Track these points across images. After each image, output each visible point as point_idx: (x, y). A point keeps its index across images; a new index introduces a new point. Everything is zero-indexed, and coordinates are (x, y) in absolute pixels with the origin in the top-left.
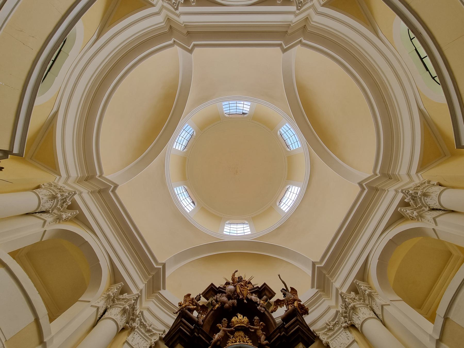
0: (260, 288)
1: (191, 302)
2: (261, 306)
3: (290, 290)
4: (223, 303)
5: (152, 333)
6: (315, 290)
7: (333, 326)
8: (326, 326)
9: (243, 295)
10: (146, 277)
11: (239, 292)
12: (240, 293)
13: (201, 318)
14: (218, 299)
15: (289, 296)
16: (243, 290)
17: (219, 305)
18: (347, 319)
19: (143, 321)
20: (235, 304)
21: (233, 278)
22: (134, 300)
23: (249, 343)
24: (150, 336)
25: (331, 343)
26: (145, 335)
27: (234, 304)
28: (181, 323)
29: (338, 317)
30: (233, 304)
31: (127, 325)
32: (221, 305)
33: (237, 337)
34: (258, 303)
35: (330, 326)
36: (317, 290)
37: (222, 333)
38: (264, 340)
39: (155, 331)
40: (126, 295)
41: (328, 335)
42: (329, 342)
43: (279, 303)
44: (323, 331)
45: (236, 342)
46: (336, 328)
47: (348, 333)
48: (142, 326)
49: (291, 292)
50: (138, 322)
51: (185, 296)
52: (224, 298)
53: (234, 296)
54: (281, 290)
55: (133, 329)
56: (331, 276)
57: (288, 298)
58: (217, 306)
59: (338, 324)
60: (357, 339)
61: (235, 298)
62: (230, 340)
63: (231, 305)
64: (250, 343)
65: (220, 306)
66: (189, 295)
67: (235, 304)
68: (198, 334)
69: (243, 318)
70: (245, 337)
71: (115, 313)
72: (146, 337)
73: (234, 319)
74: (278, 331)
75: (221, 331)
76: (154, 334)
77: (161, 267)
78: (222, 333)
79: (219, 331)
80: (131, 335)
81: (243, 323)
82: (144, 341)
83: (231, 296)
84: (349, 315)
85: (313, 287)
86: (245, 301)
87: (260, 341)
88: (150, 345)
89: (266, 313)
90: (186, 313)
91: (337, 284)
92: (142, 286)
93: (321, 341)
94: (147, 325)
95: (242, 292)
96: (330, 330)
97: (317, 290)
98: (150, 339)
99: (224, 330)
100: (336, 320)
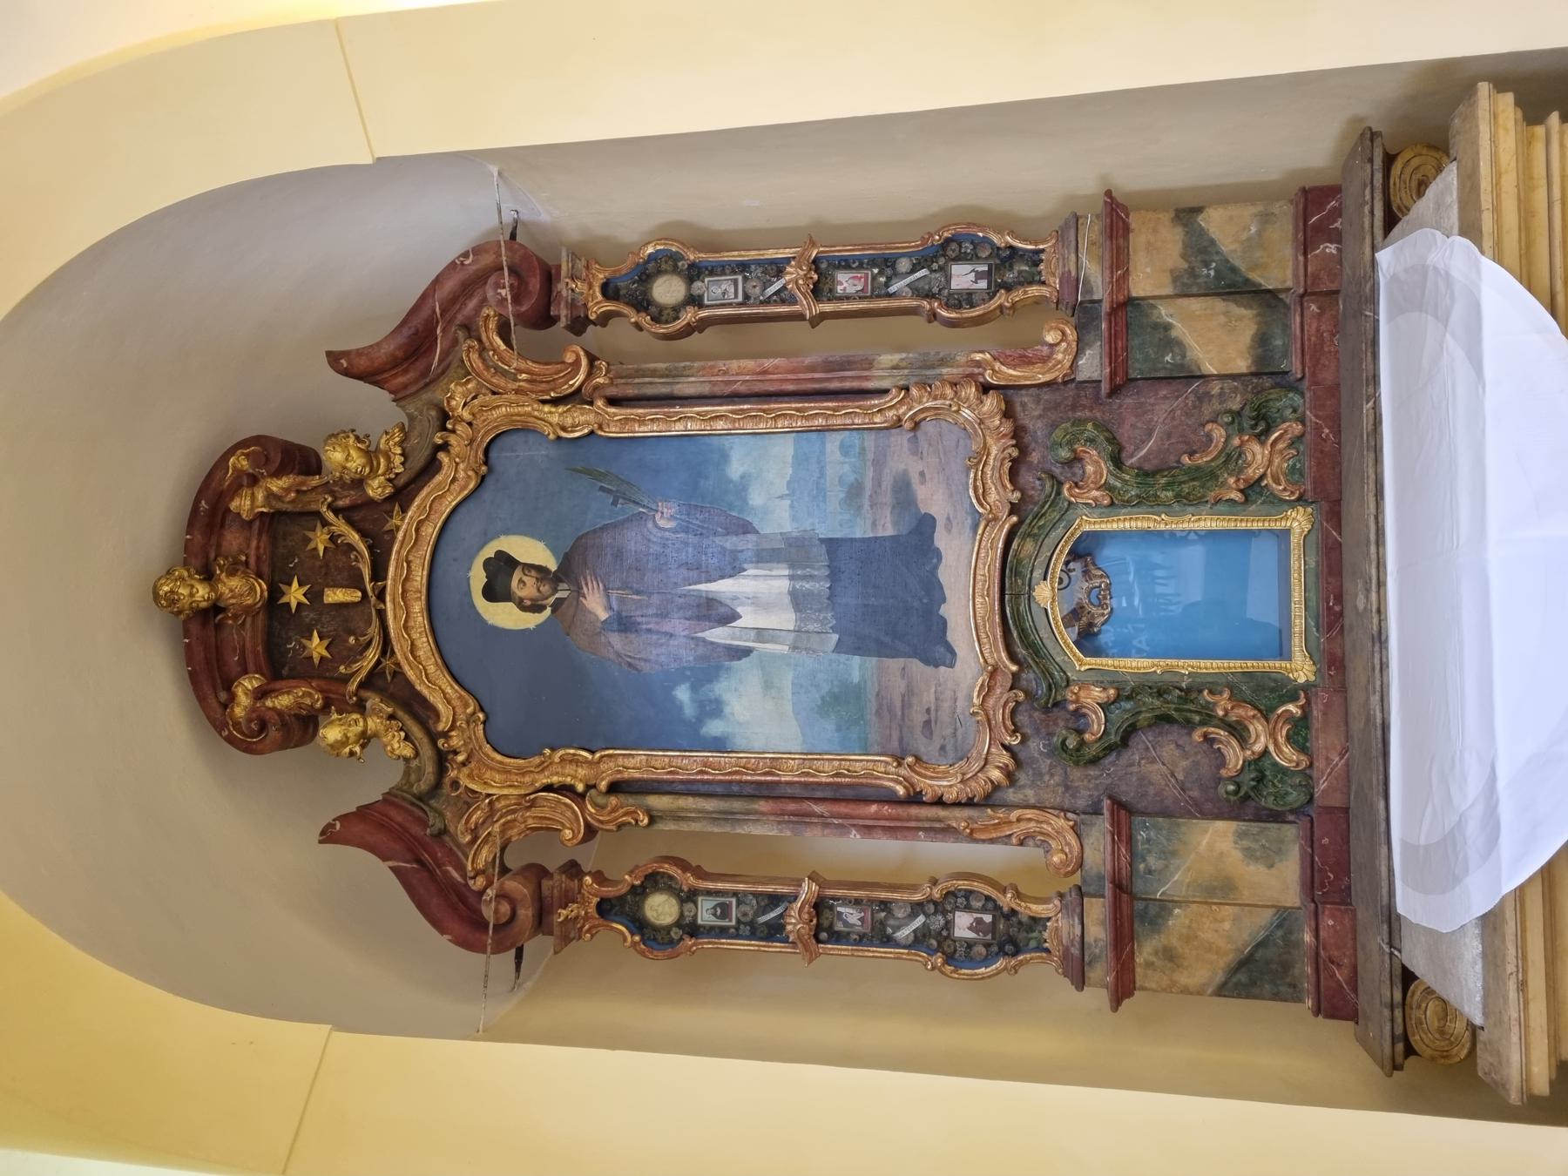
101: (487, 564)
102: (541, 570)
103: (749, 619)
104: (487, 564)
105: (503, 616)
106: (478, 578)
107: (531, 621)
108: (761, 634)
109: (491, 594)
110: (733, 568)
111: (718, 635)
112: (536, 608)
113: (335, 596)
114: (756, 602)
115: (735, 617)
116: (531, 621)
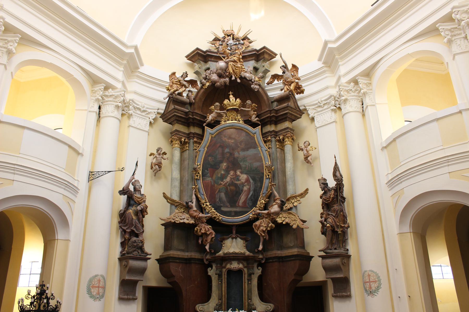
0: (258, 51)
1: (179, 84)
2: (256, 84)
3: (290, 67)
4: (213, 83)
5: (147, 112)
6: (320, 65)
7: (324, 104)
8: (318, 103)
9: (235, 73)
10: (120, 64)
11: (231, 72)
12: (233, 73)
13: (192, 96)
14: (207, 77)
15: (288, 77)
16: (237, 68)
17: (210, 83)
18: (337, 103)
19: (135, 105)
20: (228, 83)
21: (224, 50)
22: (122, 97)
23: (240, 122)
24: (146, 114)
25: (317, 117)
26: (142, 115)
27: (226, 83)
28: (175, 110)
29: (330, 100)
30: (225, 83)
31: (123, 112)
32: (211, 83)
33: (230, 116)
34: (253, 81)
35: (321, 104)
36: (323, 65)
37: (215, 114)
38: (254, 119)
39: (149, 111)
40: (110, 92)
41: (317, 110)
42: (315, 116)
43: (275, 77)
44: (313, 107)
45: (228, 120)
46: (326, 107)
47: (333, 113)
48: (136, 110)
49: (291, 69)
50: (132, 109)
51: (170, 75)
52: (214, 77)
53: (226, 73)
54: (281, 67)
55: (130, 116)
56: (342, 58)
57: (286, 78)
58: (208, 84)
59: (328, 104)
60: (338, 120)
61: (227, 76)
62: (223, 119)
63: (223, 84)
64: (241, 121)
65: (210, 84)
66: (174, 74)
67: (228, 83)
68: (193, 116)
69: (236, 100)
70: (237, 116)
71: (108, 110)
72: (144, 116)
73: (226, 102)
74: (268, 112)
75: (214, 113)
76: (149, 113)
77: (132, 51)
78: (215, 114)
79: (211, 112)
80: (131, 119)
81: (235, 106)
82: (143, 120)
83: (223, 74)
84: (340, 102)
85: (320, 60)
86: (239, 81)
87: (251, 119)
88: (149, 122)
89: (260, 90)
90: (177, 99)
91: (343, 70)
92: (120, 75)
93: (309, 115)
94: (140, 108)
95: (235, 71)
96: (320, 106)
97: (323, 65)
98: (147, 117)
99: (217, 113)
100: (328, 101)
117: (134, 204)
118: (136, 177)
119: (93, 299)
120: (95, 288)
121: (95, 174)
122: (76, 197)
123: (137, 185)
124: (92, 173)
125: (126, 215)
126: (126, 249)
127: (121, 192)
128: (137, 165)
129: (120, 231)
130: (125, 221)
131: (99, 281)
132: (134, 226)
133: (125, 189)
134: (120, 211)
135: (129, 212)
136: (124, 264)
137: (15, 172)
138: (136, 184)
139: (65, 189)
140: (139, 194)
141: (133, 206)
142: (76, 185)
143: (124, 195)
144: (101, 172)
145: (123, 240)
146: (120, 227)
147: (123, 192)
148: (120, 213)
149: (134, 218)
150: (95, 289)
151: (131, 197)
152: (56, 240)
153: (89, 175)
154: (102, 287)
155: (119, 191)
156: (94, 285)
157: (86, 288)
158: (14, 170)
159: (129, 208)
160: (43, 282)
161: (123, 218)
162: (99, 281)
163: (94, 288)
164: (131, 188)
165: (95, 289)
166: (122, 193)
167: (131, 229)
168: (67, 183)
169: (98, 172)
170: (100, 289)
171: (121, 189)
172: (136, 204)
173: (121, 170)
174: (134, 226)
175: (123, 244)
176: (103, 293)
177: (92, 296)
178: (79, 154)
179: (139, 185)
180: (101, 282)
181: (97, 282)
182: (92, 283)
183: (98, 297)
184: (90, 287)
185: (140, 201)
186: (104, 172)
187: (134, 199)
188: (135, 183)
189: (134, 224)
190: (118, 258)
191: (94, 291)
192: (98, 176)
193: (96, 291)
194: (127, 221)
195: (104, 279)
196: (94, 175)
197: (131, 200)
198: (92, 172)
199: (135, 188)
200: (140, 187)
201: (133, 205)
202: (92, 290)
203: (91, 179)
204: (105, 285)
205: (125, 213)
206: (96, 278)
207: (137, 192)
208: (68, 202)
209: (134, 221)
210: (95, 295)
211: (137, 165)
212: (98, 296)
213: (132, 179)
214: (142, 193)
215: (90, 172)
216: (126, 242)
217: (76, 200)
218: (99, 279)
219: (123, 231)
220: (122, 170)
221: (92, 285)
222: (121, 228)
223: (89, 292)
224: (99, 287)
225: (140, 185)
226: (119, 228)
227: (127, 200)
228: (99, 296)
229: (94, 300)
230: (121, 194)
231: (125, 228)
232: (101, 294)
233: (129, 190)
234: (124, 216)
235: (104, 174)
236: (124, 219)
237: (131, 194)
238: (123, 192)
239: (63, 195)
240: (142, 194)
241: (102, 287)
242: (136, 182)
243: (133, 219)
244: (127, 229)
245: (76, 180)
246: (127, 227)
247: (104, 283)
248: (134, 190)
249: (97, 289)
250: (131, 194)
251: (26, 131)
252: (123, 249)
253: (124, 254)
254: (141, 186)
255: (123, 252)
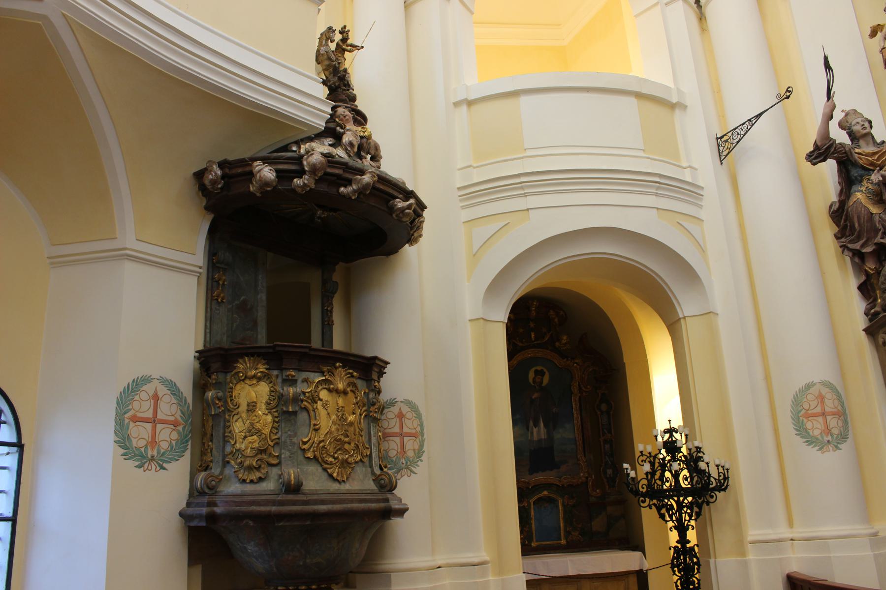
101: (542, 370)
102: (542, 383)
103: (535, 430)
104: (542, 370)
105: (531, 375)
106: (539, 368)
107: (531, 380)
108: (532, 433)
109: (536, 372)
110: (545, 426)
111: (531, 423)
112: (534, 382)
113: (533, 335)
114: (539, 432)
115: (535, 427)
116: (531, 380)
117: (862, 176)
118: (843, 103)
119: (817, 448)
120: (815, 418)
121: (730, 138)
122: (701, 207)
123: (853, 123)
124: (723, 140)
125: (850, 209)
126: (879, 300)
127: (813, 157)
128: (827, 66)
129: (848, 259)
130: (852, 227)
131: (821, 398)
132: (880, 233)
133: (819, 144)
134: (831, 207)
135: (855, 199)
136: (881, 341)
137: (526, 191)
138: (850, 121)
139: (657, 195)
140: (868, 144)
141: (861, 181)
142: (689, 179)
143: (824, 160)
144: (741, 127)
145: (863, 278)
146: (844, 247)
147: (819, 154)
148: (832, 210)
149: (874, 210)
150: (815, 422)
151: (848, 159)
152: (682, 321)
153: (719, 146)
154: (833, 414)
155: (807, 155)
156: (808, 410)
157: (791, 420)
158: (522, 188)
159: (852, 190)
160: (670, 423)
161: (845, 221)
162: (821, 398)
163: (810, 419)
164: (840, 137)
165: (815, 422)
166: (815, 159)
167: (876, 244)
168: (657, 179)
169: (735, 129)
170: (829, 418)
171: (812, 149)
172: (867, 173)
173: (785, 96)
174: (880, 233)
175: (865, 289)
176: (842, 429)
177: (811, 441)
178: (673, 106)
179: (859, 120)
180: (826, 400)
181: (815, 402)
182: (802, 405)
183: (828, 441)
184: (801, 418)
185: (878, 159)
186: (747, 123)
187: (856, 161)
188: (847, 122)
189: (881, 227)
190: (864, 330)
191: (815, 427)
192: (737, 140)
193: (819, 426)
194: (856, 225)
195: (834, 389)
196: (729, 140)
197: (850, 167)
198: (721, 138)
199: (852, 135)
200: (867, 124)
201: (860, 178)
202: (809, 425)
203: (724, 153)
204: (843, 407)
205: (846, 208)
206: (808, 392)
207: (862, 143)
208: (677, 222)
209: (877, 218)
210: (819, 437)
211: (827, 66)
212: (828, 439)
213: (828, 110)
214: (878, 141)
215: (717, 139)
216: (874, 281)
217: (702, 214)
218: (820, 392)
219: (854, 254)
220: (788, 94)
221: (804, 411)
222: (849, 249)
223: (801, 430)
224: (824, 414)
225: (862, 121)
226: (840, 250)
227: (840, 171)
228: (832, 435)
229: (820, 449)
230: (814, 161)
231: (857, 246)
232: (835, 431)
233: (831, 142)
234: (843, 217)
235: (749, 127)
236: (848, 222)
237: (845, 153)
238: (819, 154)
239: (657, 209)
240: (878, 141)
241: (833, 414)
242: (849, 117)
243: (872, 214)
244: (863, 246)
245: (685, 169)
246: (861, 242)
247: (836, 402)
248: (852, 140)
249: (820, 419)
250: (845, 153)
251: (524, 100)
252: (870, 301)
253: (876, 314)
254: (870, 122)
255: (873, 311)
